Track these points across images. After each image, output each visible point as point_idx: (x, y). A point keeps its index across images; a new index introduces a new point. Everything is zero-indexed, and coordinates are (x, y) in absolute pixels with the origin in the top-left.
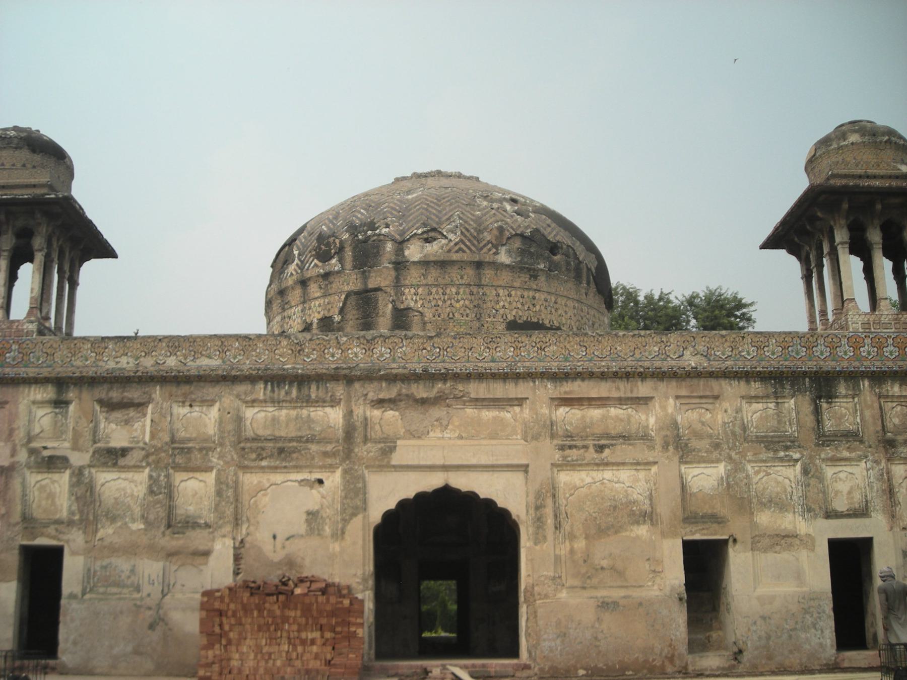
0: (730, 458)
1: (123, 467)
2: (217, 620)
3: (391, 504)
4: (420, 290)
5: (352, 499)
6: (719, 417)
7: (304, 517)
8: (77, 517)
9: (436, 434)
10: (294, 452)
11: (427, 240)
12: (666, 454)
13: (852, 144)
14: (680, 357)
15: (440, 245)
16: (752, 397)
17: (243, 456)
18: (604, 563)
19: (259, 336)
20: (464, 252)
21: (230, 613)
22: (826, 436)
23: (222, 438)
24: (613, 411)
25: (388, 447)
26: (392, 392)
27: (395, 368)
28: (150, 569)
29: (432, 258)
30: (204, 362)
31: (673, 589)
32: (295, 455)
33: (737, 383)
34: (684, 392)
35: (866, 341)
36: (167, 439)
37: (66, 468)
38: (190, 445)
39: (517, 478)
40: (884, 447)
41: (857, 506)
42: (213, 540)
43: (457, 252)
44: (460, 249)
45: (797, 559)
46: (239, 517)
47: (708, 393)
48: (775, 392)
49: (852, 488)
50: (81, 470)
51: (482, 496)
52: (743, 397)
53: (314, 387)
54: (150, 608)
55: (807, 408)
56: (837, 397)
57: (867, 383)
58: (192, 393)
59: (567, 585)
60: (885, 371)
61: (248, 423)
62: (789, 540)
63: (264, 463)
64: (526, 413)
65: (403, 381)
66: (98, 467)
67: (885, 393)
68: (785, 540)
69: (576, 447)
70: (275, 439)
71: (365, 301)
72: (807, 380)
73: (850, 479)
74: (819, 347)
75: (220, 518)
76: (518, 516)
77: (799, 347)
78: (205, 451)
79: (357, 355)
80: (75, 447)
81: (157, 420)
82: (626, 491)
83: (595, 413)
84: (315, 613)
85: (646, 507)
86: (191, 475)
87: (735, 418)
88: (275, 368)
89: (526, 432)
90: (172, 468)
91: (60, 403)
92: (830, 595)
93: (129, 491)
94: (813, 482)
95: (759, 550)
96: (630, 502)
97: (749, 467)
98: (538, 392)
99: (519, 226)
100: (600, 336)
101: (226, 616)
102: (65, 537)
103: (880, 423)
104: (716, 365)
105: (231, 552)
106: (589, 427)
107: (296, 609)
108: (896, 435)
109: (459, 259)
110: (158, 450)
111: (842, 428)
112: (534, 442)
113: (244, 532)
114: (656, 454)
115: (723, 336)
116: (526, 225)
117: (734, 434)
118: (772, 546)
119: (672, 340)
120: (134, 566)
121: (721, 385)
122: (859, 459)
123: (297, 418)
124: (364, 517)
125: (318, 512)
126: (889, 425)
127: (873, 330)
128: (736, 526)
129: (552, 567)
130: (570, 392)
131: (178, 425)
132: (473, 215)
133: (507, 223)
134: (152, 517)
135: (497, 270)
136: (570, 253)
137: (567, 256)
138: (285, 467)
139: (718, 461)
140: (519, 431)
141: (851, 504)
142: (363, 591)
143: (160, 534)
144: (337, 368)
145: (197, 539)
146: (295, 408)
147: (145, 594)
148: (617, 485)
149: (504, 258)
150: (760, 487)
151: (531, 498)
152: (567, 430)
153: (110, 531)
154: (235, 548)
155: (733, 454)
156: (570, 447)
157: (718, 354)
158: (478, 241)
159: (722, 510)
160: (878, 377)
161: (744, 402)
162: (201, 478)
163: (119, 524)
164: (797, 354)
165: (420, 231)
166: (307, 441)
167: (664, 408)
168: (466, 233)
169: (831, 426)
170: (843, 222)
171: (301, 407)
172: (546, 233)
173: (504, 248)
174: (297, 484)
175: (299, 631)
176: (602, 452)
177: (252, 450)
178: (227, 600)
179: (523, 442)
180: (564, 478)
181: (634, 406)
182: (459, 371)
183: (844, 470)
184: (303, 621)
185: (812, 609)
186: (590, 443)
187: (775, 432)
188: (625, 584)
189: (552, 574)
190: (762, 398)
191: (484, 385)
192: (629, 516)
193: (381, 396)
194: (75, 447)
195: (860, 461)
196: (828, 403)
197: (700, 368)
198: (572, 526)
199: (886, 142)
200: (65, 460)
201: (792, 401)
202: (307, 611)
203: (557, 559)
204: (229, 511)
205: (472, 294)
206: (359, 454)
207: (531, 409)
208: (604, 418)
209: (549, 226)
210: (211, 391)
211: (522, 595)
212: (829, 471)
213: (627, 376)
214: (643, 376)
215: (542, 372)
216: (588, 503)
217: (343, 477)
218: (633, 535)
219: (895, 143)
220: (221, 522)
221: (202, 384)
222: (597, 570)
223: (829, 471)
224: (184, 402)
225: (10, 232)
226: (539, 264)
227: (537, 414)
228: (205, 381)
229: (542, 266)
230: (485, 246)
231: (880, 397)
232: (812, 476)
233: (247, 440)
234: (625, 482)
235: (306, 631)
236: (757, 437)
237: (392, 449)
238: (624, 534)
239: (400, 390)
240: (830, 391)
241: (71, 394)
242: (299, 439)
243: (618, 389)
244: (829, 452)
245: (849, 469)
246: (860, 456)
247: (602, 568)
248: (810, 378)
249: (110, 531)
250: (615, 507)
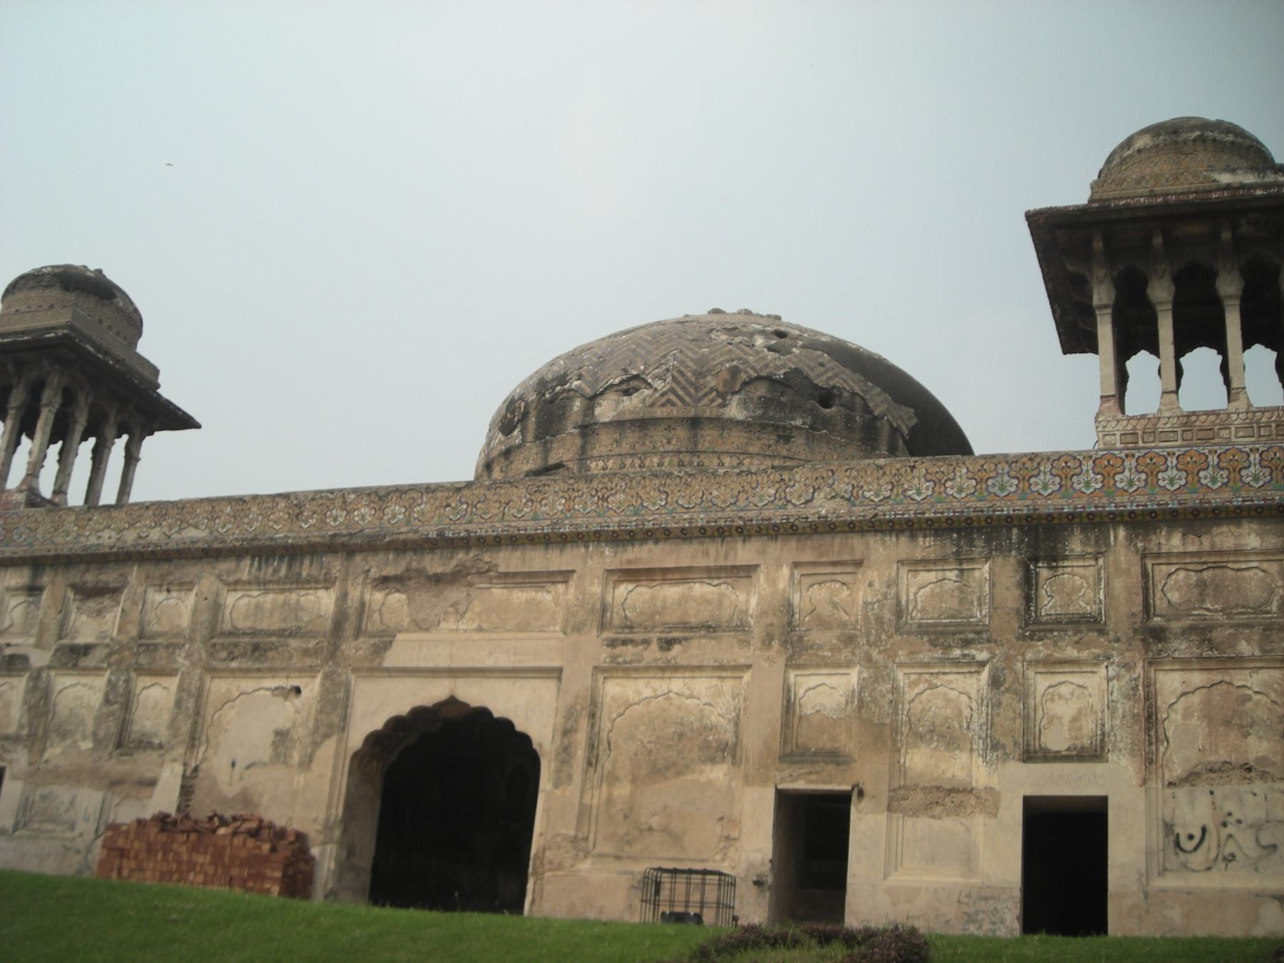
0: (869, 659)
1: (84, 669)
2: (117, 862)
3: (378, 723)
4: (610, 463)
5: (328, 714)
6: (861, 594)
7: (271, 738)
8: (25, 732)
9: (450, 624)
10: (270, 649)
11: (627, 393)
12: (767, 653)
13: (1139, 151)
14: (807, 502)
15: (641, 397)
16: (917, 562)
17: (212, 655)
18: (655, 822)
19: (255, 497)
20: (673, 404)
21: (132, 855)
22: (1040, 623)
23: (193, 631)
24: (699, 589)
26: (394, 567)
27: (405, 533)
29: (627, 417)
30: (191, 533)
31: (751, 866)
32: (270, 654)
33: (894, 539)
34: (807, 557)
35: (1127, 463)
36: (133, 631)
37: (26, 670)
38: (159, 640)
39: (547, 688)
40: (1143, 640)
41: (1086, 742)
42: (162, 765)
43: (663, 405)
44: (669, 401)
45: (968, 830)
46: (197, 735)
47: (846, 557)
48: (958, 553)
49: (1080, 710)
50: (40, 670)
51: (496, 714)
52: (901, 562)
53: (307, 562)
54: (78, 852)
56: (1066, 558)
57: (1122, 533)
58: (169, 573)
59: (597, 851)
60: (1153, 511)
61: (227, 611)
62: (960, 797)
63: (234, 664)
64: (566, 594)
65: (415, 551)
66: (59, 668)
67: (1155, 550)
68: (951, 796)
69: (632, 641)
70: (255, 633)
72: (1015, 531)
73: (1077, 696)
74: (1042, 477)
75: (175, 736)
76: (540, 745)
77: (1006, 478)
78: (172, 647)
80: (38, 645)
81: (127, 609)
82: (701, 711)
83: (672, 592)
84: (227, 860)
85: (729, 737)
86: (154, 680)
87: (885, 596)
89: (567, 621)
90: (135, 670)
91: (33, 590)
92: (1017, 893)
93: (86, 700)
94: (1007, 699)
95: (904, 812)
96: (705, 727)
97: (900, 675)
98: (590, 562)
99: (767, 366)
100: (690, 475)
101: (128, 858)
102: (9, 757)
103: (1139, 599)
105: (179, 782)
106: (659, 613)
107: (206, 853)
108: (1169, 620)
109: (665, 415)
110: (123, 647)
111: (1072, 609)
112: (575, 635)
113: (200, 756)
114: (750, 653)
115: (881, 468)
116: (778, 365)
117: (879, 620)
118: (926, 809)
119: (797, 477)
120: (74, 797)
121: (867, 544)
122: (1096, 661)
123: (283, 605)
124: (340, 740)
125: (288, 731)
126: (1160, 603)
127: (1141, 444)
128: (868, 771)
129: (574, 822)
130: (637, 560)
131: (151, 616)
132: (695, 353)
133: (746, 362)
134: (101, 733)
135: (723, 429)
136: (854, 404)
137: (849, 407)
138: (258, 670)
139: (848, 664)
140: (559, 620)
141: (1076, 738)
142: (324, 843)
143: (106, 755)
144: (335, 535)
145: (144, 763)
146: (283, 591)
147: (76, 833)
148: (689, 702)
149: (735, 410)
150: (917, 706)
151: (561, 715)
152: (626, 617)
153: (58, 750)
154: (184, 777)
155: (874, 653)
156: (624, 642)
157: (867, 494)
158: (697, 389)
159: (847, 742)
161: (904, 571)
162: (165, 685)
163: (69, 742)
164: (1002, 489)
165: (617, 381)
166: (289, 636)
167: (772, 581)
168: (680, 378)
169: (1054, 607)
170: (1100, 273)
171: (291, 590)
172: (812, 375)
173: (736, 397)
174: (269, 693)
175: (204, 883)
176: (669, 650)
177: (224, 647)
178: (132, 836)
179: (561, 635)
180: (613, 689)
181: (729, 580)
182: (483, 533)
184: (211, 870)
185: (981, 916)
186: (654, 636)
187: (953, 617)
188: (680, 855)
189: (572, 833)
190: (935, 562)
191: (518, 553)
192: (701, 749)
193: (385, 573)
194: (38, 645)
195: (1096, 665)
196: (1050, 568)
197: (831, 517)
198: (614, 763)
199: (1195, 140)
200: (25, 659)
201: (987, 567)
202: (217, 857)
203: (584, 813)
204: (185, 728)
205: (681, 464)
206: (347, 652)
207: (577, 587)
208: (683, 600)
209: (822, 365)
210: (191, 570)
211: (531, 863)
213: (721, 533)
214: (745, 532)
215: (596, 532)
216: (642, 728)
217: (322, 685)
218: (703, 779)
219: (1214, 140)
220: (174, 742)
221: (183, 562)
222: (642, 831)
223: (1041, 683)
224: (160, 586)
225: (21, 386)
226: (793, 419)
227: (584, 594)
228: (186, 558)
229: (799, 422)
230: (706, 395)
231: (1144, 556)
232: (1007, 690)
233: (223, 634)
234: (702, 697)
235: (212, 883)
236: (920, 625)
237: (387, 646)
238: (689, 777)
239: (410, 563)
240: (1054, 548)
241: (45, 579)
242: (281, 633)
243: (707, 554)
244: (1041, 649)
245: (1077, 679)
246: (1096, 657)
247: (650, 829)
248: (1021, 528)
249: (58, 750)
250: (681, 736)
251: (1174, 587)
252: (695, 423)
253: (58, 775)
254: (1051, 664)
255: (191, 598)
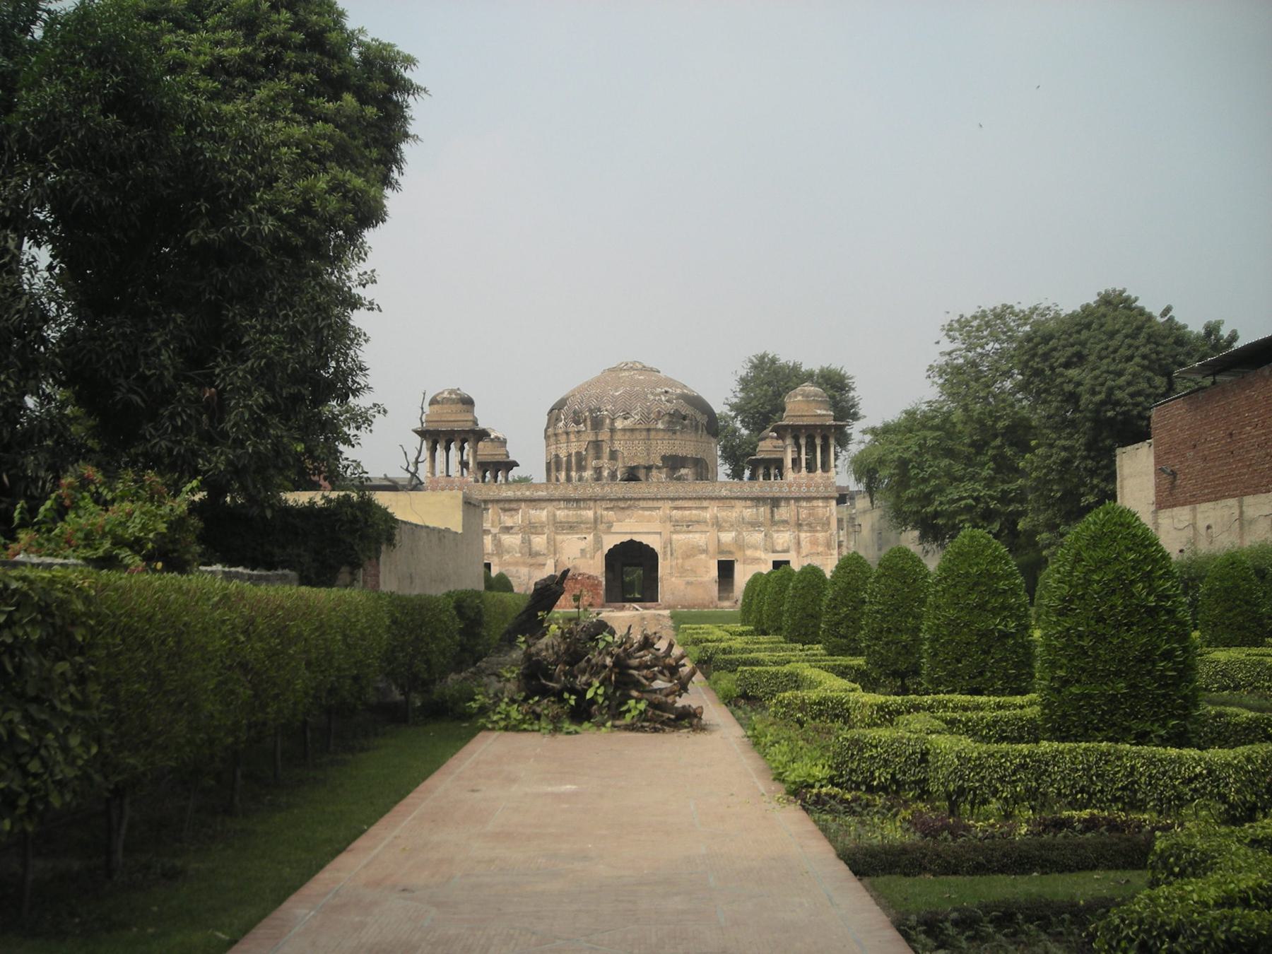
25: (610, 527)
28: (524, 571)
55: (768, 511)
71: (597, 445)
73: (783, 538)
78: (542, 527)
79: (598, 490)
83: (687, 513)
88: (567, 496)
104: (734, 495)
128: (736, 556)
145: (540, 559)
149: (660, 426)
160: (797, 499)
180: (675, 537)
183: (781, 535)
202: (583, 585)
210: (543, 504)
212: (775, 535)
223: (775, 535)
234: (698, 538)
251: (804, 514)
252: (648, 430)
253: (509, 564)
254: (778, 531)
255: (545, 513)
